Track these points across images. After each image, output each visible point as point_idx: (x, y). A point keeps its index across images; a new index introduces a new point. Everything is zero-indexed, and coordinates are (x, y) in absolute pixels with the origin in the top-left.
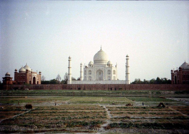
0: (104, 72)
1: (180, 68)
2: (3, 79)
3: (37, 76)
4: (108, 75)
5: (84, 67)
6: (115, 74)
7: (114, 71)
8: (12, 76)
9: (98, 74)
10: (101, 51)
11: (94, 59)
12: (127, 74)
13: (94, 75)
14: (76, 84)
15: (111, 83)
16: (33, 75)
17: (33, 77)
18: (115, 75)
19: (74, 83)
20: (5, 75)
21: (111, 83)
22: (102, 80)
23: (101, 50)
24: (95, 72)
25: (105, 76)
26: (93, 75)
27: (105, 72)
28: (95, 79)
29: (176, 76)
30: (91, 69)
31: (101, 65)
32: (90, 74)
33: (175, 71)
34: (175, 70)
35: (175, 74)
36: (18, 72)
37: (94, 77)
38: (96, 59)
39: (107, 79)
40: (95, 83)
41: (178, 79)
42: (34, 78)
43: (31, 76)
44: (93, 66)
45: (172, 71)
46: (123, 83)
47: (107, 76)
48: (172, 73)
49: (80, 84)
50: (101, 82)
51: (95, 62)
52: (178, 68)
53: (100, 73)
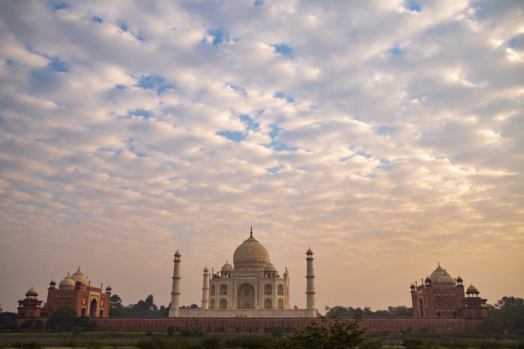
0: (256, 289)
1: (427, 280)
2: (20, 305)
3: (101, 299)
4: (267, 297)
5: (211, 278)
7: (280, 286)
8: (43, 297)
9: (244, 294)
10: (251, 239)
12: (310, 293)
13: (233, 296)
14: (189, 316)
16: (92, 295)
17: (92, 299)
19: (184, 315)
20: (26, 295)
21: (273, 315)
22: (254, 308)
23: (251, 237)
24: (236, 290)
25: (258, 300)
26: (232, 296)
27: (258, 288)
28: (235, 306)
29: (420, 298)
30: (228, 283)
32: (225, 294)
33: (419, 288)
34: (419, 284)
35: (420, 294)
36: (57, 287)
37: (233, 301)
39: (263, 305)
40: (233, 316)
41: (426, 306)
42: (94, 302)
43: (87, 298)
44: (232, 275)
45: (412, 287)
46: (299, 316)
48: (412, 292)
50: (250, 312)
51: (237, 265)
52: (424, 280)
53: (247, 293)
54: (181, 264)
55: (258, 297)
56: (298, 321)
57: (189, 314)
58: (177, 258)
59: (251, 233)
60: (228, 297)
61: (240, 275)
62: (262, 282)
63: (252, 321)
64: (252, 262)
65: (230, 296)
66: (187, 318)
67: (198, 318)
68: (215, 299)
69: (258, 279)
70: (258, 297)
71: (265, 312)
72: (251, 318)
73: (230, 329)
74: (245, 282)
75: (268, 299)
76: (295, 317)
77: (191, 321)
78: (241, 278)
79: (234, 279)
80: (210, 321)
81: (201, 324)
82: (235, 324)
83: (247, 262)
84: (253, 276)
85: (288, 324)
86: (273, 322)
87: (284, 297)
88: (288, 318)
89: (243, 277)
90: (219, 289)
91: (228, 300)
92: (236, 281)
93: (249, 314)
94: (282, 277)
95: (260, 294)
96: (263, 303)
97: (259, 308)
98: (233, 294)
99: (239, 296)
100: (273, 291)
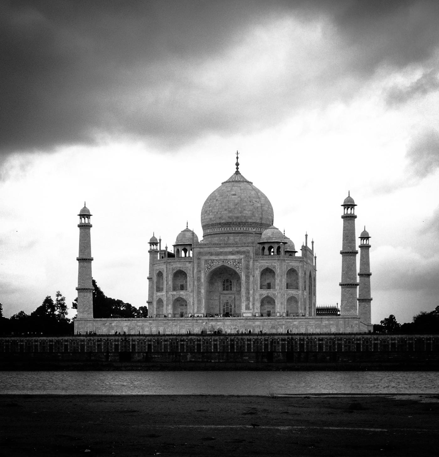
0: (243, 278)
4: (265, 292)
6: (298, 289)
9: (221, 289)
11: (202, 220)
13: (199, 292)
15: (274, 331)
18: (292, 292)
21: (273, 327)
22: (239, 315)
23: (237, 173)
25: (248, 299)
26: (195, 292)
27: (247, 277)
28: (203, 311)
30: (187, 267)
31: (227, 245)
32: (182, 288)
37: (199, 301)
38: (211, 219)
40: (197, 330)
46: (325, 330)
47: (257, 297)
49: (132, 333)
50: (228, 323)
51: (208, 231)
54: (93, 231)
55: (248, 293)
56: (322, 340)
57: (112, 328)
58: (85, 221)
59: (237, 164)
60: (189, 295)
61: (212, 250)
62: (257, 264)
63: (231, 340)
64: (240, 224)
65: (192, 291)
66: (109, 335)
67: (129, 335)
68: (164, 299)
69: (247, 257)
70: (248, 293)
71: (258, 323)
72: (230, 335)
73: (189, 356)
74: (221, 264)
75: (268, 297)
76: (318, 331)
77: (115, 341)
78: (213, 257)
79: (199, 259)
80: (150, 341)
81: (134, 346)
82: (199, 345)
83: (228, 224)
84: (238, 252)
85: (302, 345)
86: (272, 342)
87: (300, 292)
88: (302, 334)
89: (218, 254)
90: (170, 277)
91: (190, 300)
92: (203, 262)
93: (228, 326)
94: (299, 254)
95: (251, 287)
96: (258, 305)
97: (250, 315)
98: (199, 288)
99: (209, 292)
100: (277, 281)
